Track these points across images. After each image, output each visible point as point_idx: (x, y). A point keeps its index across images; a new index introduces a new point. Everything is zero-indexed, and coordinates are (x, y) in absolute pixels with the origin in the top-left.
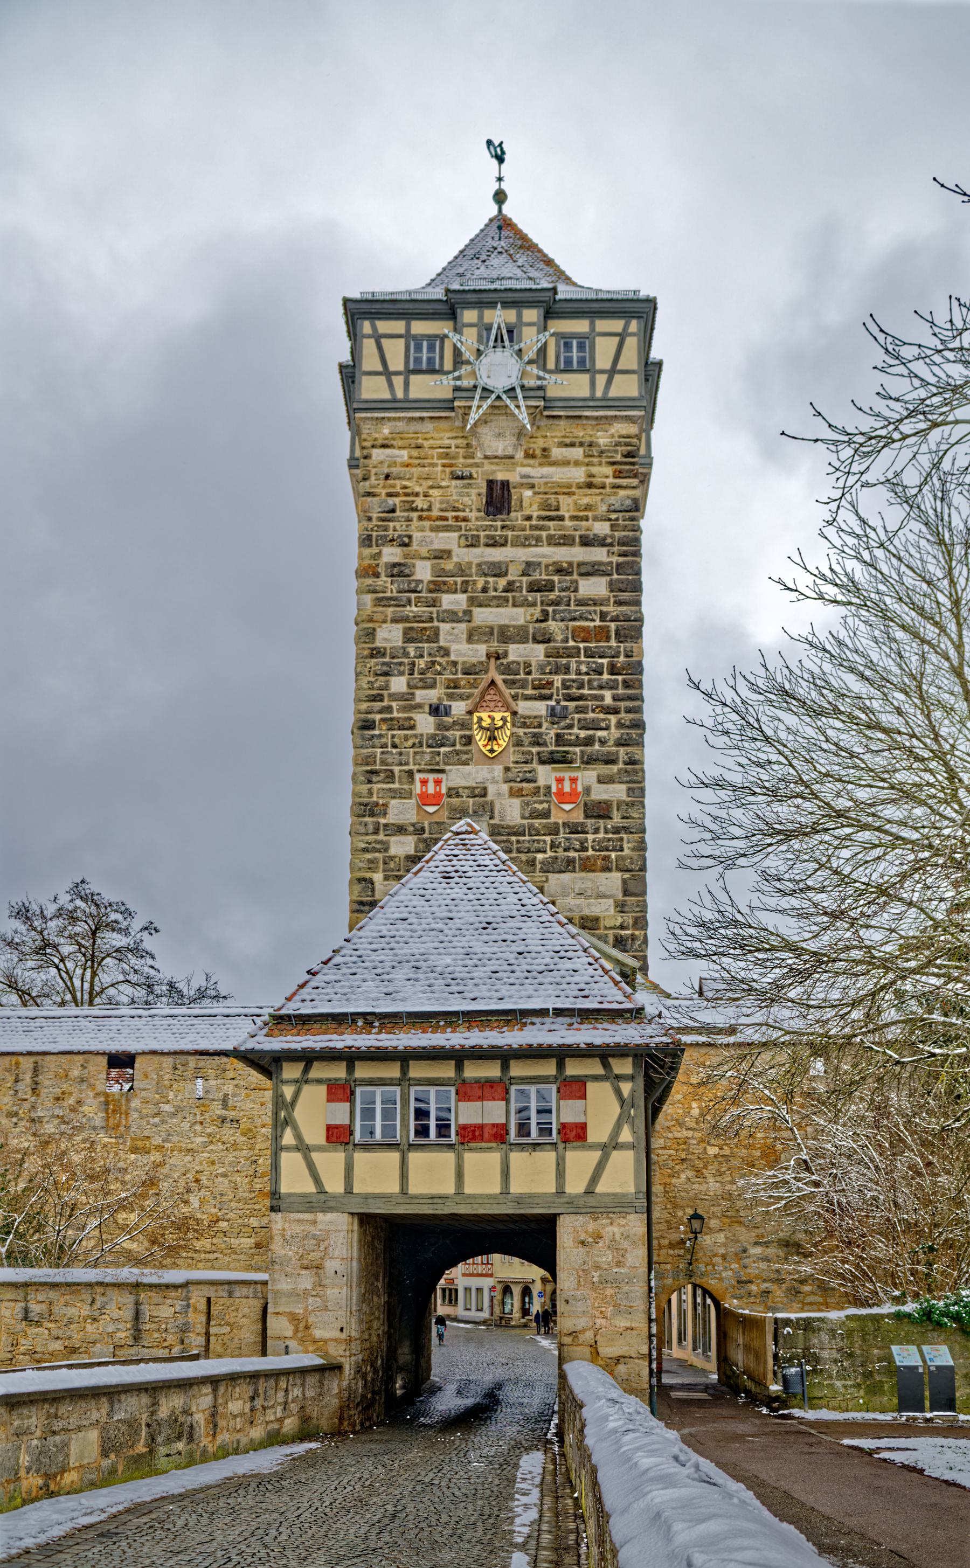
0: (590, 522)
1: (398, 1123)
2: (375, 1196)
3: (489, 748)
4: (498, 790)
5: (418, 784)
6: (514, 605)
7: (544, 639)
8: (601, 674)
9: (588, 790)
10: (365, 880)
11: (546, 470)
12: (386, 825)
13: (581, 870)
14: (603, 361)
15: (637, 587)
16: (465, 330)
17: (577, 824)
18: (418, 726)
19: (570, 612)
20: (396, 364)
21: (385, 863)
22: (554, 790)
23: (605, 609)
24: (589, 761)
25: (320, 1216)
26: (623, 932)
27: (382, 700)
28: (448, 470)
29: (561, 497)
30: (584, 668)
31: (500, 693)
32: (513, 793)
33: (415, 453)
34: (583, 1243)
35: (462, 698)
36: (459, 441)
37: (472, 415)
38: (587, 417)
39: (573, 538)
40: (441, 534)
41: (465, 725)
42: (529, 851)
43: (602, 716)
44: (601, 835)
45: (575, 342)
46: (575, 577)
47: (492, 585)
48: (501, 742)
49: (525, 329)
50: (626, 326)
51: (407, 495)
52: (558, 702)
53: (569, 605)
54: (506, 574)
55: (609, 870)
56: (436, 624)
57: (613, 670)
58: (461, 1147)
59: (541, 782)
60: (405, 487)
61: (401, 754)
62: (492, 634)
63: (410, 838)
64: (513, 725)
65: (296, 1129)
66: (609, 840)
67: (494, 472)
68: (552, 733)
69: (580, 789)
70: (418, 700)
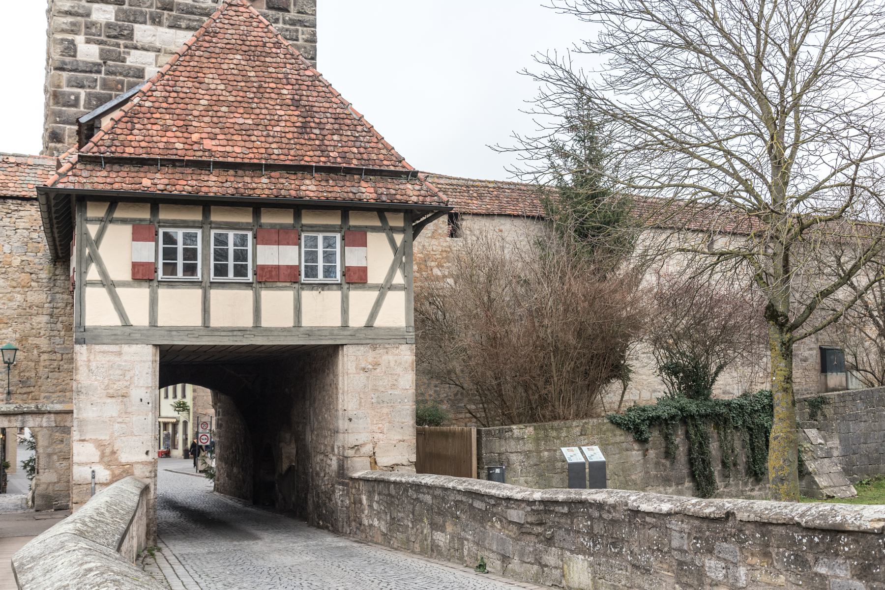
10: (66, 40)
21: (87, 27)
44: (280, 25)
58: (259, 286)
65: (100, 264)
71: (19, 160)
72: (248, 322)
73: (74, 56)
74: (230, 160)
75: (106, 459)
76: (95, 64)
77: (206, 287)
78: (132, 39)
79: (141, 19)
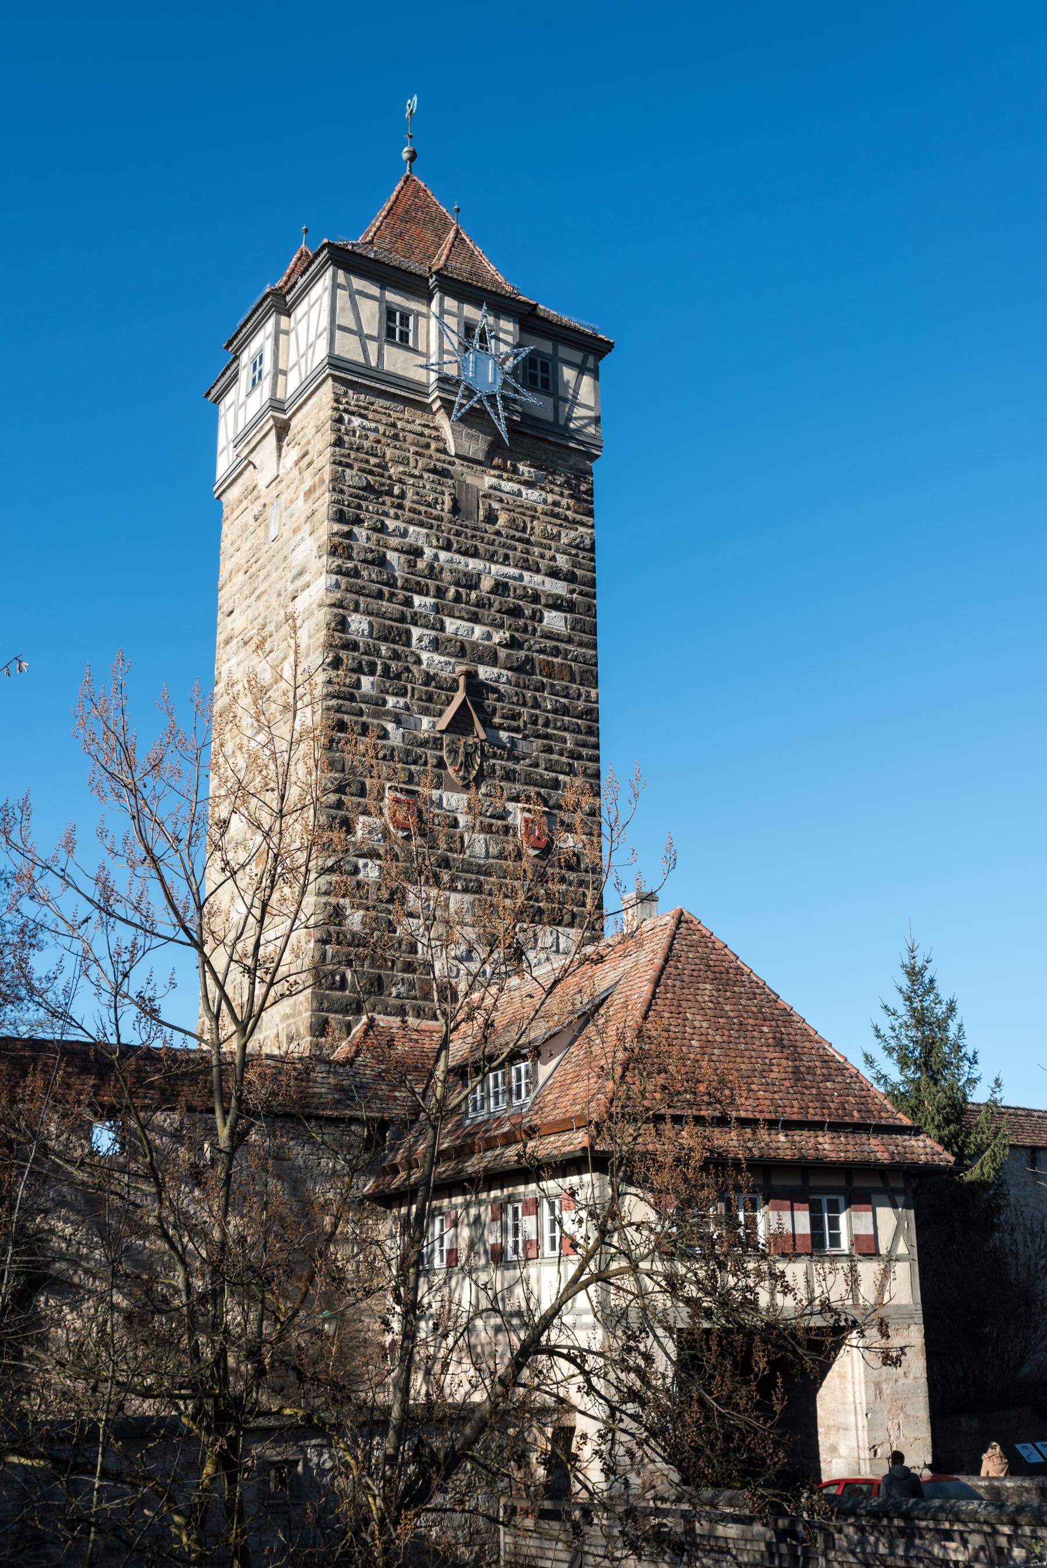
55: (571, 925)
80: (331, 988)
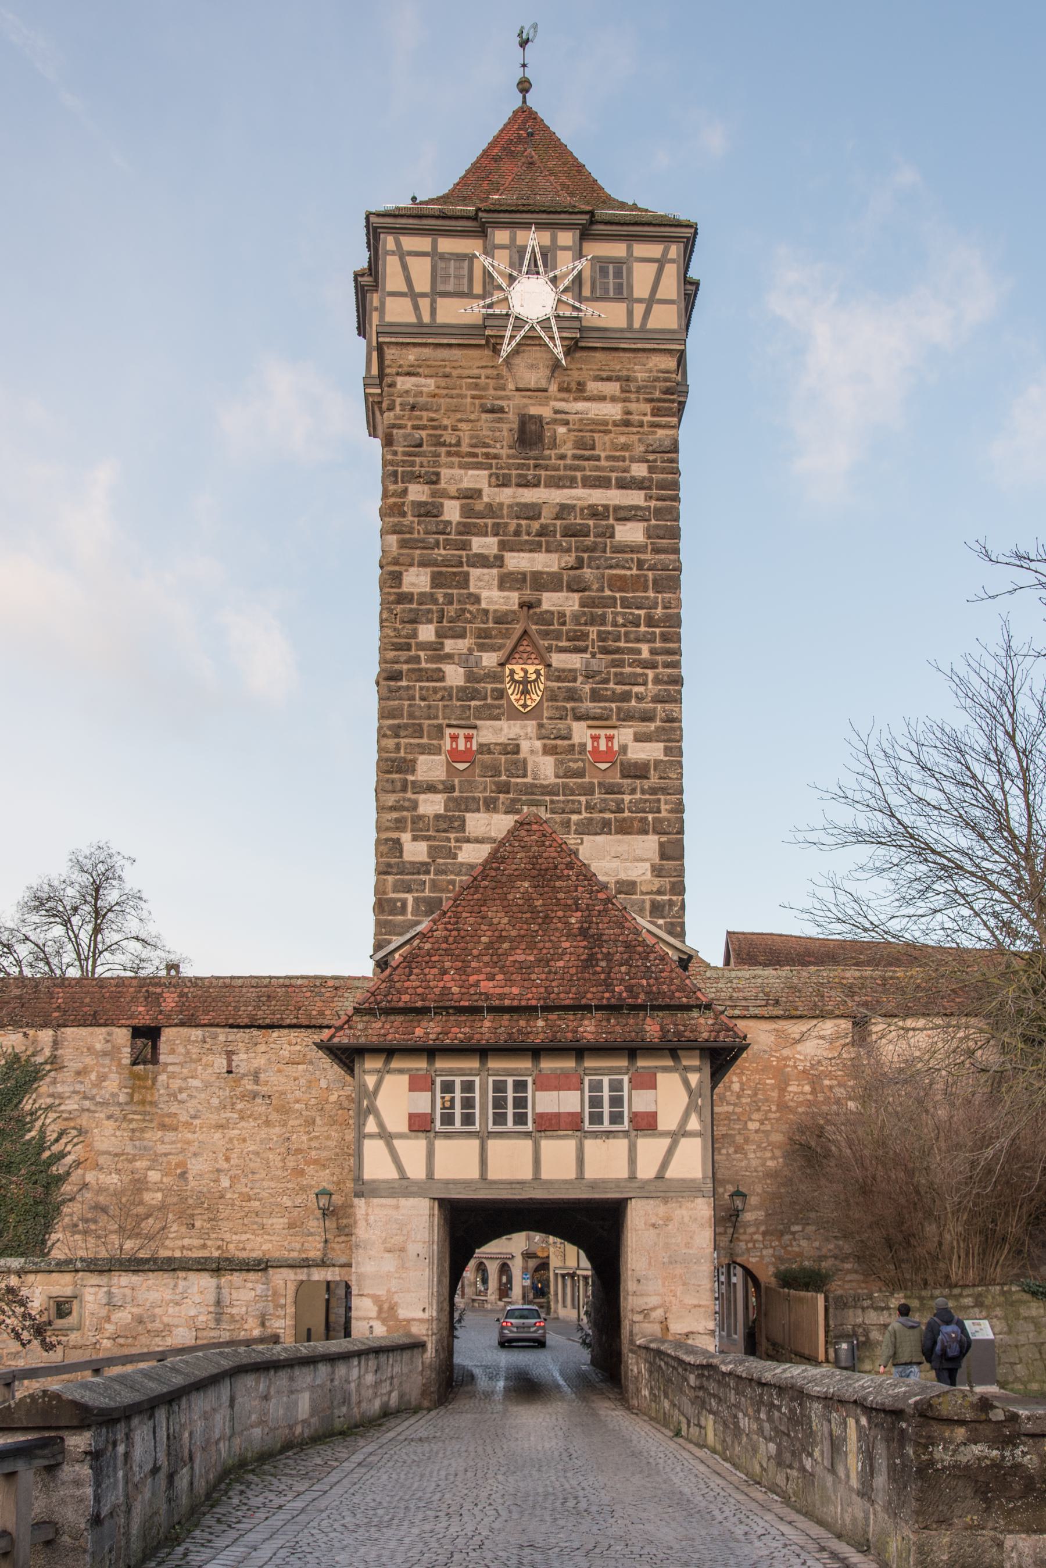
0: (627, 463)
1: (477, 1111)
2: (455, 1182)
3: (522, 702)
4: (530, 746)
5: (448, 740)
6: (548, 551)
7: (576, 586)
8: (638, 626)
9: (624, 749)
10: (391, 839)
11: (581, 406)
12: (413, 782)
13: (617, 833)
14: (641, 288)
15: (675, 533)
16: (498, 253)
17: (612, 785)
18: (447, 678)
19: (607, 559)
20: (422, 285)
21: (413, 823)
22: (589, 748)
23: (642, 557)
24: (627, 717)
25: (403, 1201)
26: (659, 898)
27: (409, 650)
28: (477, 401)
29: (596, 435)
30: (620, 620)
31: (535, 645)
32: (547, 751)
33: (443, 382)
34: (653, 1225)
35: (493, 649)
36: (489, 371)
37: (504, 347)
38: (624, 350)
39: (609, 479)
40: (470, 472)
41: (495, 677)
42: (563, 812)
43: (639, 670)
44: (638, 796)
45: (611, 267)
46: (611, 521)
47: (526, 529)
48: (534, 696)
49: (559, 253)
50: (666, 252)
51: (434, 428)
52: (593, 655)
53: (605, 552)
54: (539, 518)
55: (644, 832)
56: (466, 568)
57: (651, 622)
59: (576, 739)
60: (432, 420)
61: (429, 707)
62: (524, 580)
63: (440, 796)
64: (547, 679)
66: (646, 801)
67: (526, 406)
68: (587, 688)
69: (616, 748)
70: (447, 649)
71: (337, 983)
72: (527, 1174)
73: (401, 857)
74: (507, 1002)
75: (384, 1315)
76: (423, 864)
77: (484, 1137)
78: (464, 831)
79: (473, 806)
80: (392, 913)
